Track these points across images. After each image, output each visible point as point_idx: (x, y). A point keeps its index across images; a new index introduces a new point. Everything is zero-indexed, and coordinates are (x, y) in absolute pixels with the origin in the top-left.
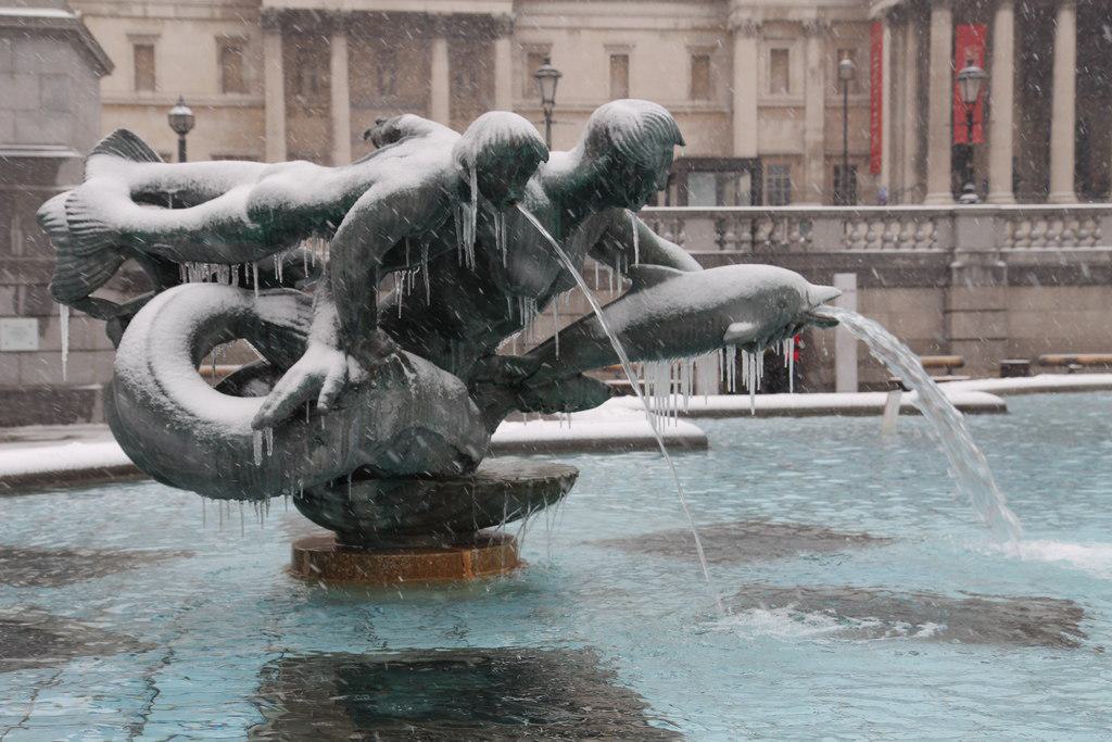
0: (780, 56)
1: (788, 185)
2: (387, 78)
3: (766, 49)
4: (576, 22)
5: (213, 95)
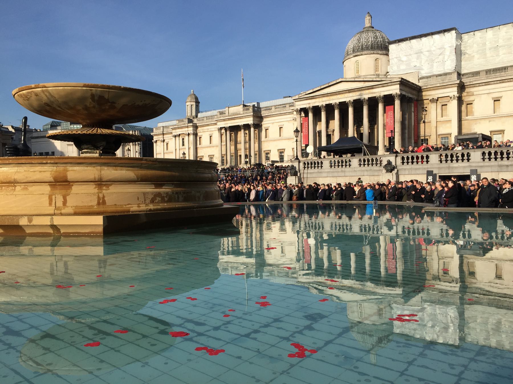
4: (273, 122)
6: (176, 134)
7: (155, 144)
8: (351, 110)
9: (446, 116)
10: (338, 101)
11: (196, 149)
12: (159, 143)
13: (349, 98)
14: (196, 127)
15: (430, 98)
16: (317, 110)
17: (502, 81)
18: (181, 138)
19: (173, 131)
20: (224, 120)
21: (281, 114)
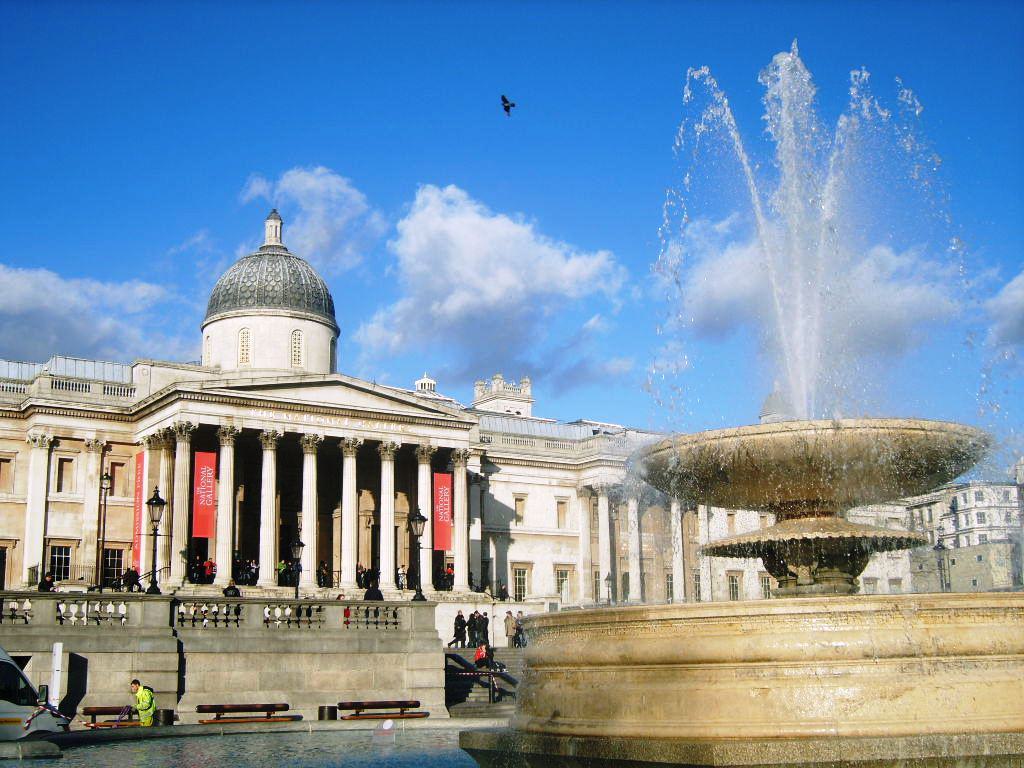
8: (350, 466)
13: (353, 431)
16: (249, 445)
17: (530, 464)
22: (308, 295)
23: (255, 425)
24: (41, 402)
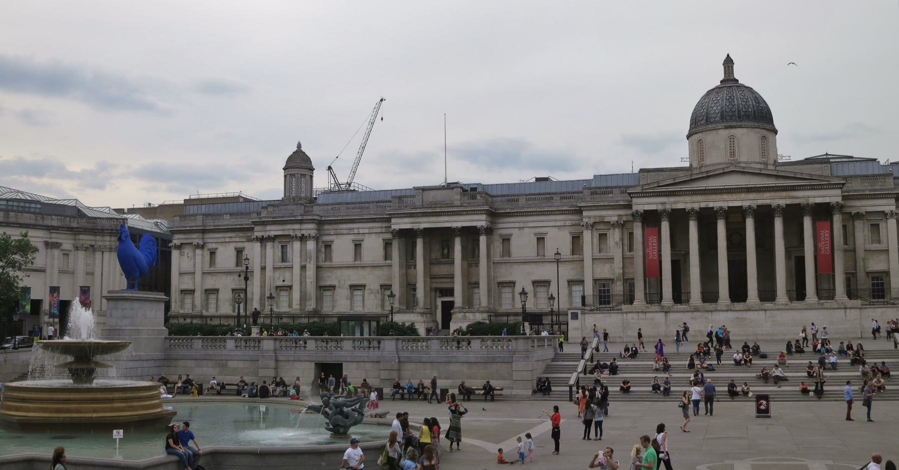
0: (603, 237)
1: (608, 290)
2: (446, 251)
3: (596, 234)
4: (522, 225)
5: (381, 261)
6: (259, 234)
7: (175, 254)
8: (750, 223)
9: (879, 242)
10: (725, 205)
11: (318, 268)
12: (187, 251)
14: (320, 223)
15: (854, 211)
16: (679, 219)
18: (278, 246)
19: (256, 228)
20: (411, 215)
21: (543, 213)
22: (739, 111)
23: (680, 206)
24: (583, 204)
